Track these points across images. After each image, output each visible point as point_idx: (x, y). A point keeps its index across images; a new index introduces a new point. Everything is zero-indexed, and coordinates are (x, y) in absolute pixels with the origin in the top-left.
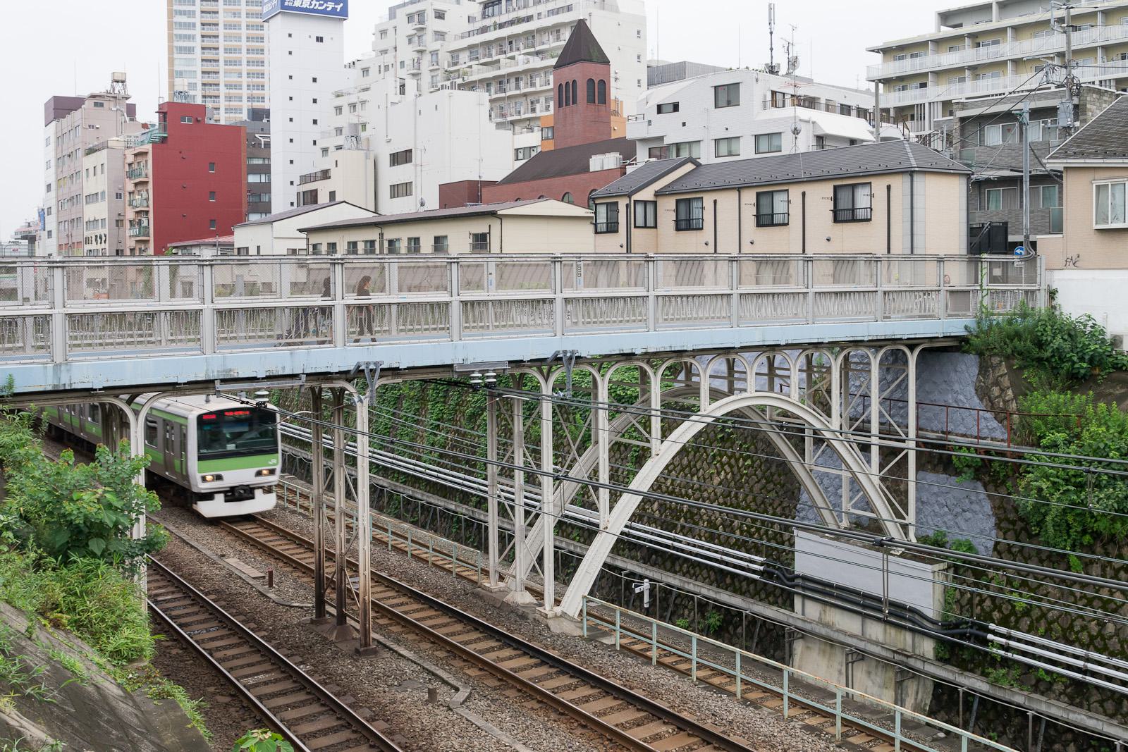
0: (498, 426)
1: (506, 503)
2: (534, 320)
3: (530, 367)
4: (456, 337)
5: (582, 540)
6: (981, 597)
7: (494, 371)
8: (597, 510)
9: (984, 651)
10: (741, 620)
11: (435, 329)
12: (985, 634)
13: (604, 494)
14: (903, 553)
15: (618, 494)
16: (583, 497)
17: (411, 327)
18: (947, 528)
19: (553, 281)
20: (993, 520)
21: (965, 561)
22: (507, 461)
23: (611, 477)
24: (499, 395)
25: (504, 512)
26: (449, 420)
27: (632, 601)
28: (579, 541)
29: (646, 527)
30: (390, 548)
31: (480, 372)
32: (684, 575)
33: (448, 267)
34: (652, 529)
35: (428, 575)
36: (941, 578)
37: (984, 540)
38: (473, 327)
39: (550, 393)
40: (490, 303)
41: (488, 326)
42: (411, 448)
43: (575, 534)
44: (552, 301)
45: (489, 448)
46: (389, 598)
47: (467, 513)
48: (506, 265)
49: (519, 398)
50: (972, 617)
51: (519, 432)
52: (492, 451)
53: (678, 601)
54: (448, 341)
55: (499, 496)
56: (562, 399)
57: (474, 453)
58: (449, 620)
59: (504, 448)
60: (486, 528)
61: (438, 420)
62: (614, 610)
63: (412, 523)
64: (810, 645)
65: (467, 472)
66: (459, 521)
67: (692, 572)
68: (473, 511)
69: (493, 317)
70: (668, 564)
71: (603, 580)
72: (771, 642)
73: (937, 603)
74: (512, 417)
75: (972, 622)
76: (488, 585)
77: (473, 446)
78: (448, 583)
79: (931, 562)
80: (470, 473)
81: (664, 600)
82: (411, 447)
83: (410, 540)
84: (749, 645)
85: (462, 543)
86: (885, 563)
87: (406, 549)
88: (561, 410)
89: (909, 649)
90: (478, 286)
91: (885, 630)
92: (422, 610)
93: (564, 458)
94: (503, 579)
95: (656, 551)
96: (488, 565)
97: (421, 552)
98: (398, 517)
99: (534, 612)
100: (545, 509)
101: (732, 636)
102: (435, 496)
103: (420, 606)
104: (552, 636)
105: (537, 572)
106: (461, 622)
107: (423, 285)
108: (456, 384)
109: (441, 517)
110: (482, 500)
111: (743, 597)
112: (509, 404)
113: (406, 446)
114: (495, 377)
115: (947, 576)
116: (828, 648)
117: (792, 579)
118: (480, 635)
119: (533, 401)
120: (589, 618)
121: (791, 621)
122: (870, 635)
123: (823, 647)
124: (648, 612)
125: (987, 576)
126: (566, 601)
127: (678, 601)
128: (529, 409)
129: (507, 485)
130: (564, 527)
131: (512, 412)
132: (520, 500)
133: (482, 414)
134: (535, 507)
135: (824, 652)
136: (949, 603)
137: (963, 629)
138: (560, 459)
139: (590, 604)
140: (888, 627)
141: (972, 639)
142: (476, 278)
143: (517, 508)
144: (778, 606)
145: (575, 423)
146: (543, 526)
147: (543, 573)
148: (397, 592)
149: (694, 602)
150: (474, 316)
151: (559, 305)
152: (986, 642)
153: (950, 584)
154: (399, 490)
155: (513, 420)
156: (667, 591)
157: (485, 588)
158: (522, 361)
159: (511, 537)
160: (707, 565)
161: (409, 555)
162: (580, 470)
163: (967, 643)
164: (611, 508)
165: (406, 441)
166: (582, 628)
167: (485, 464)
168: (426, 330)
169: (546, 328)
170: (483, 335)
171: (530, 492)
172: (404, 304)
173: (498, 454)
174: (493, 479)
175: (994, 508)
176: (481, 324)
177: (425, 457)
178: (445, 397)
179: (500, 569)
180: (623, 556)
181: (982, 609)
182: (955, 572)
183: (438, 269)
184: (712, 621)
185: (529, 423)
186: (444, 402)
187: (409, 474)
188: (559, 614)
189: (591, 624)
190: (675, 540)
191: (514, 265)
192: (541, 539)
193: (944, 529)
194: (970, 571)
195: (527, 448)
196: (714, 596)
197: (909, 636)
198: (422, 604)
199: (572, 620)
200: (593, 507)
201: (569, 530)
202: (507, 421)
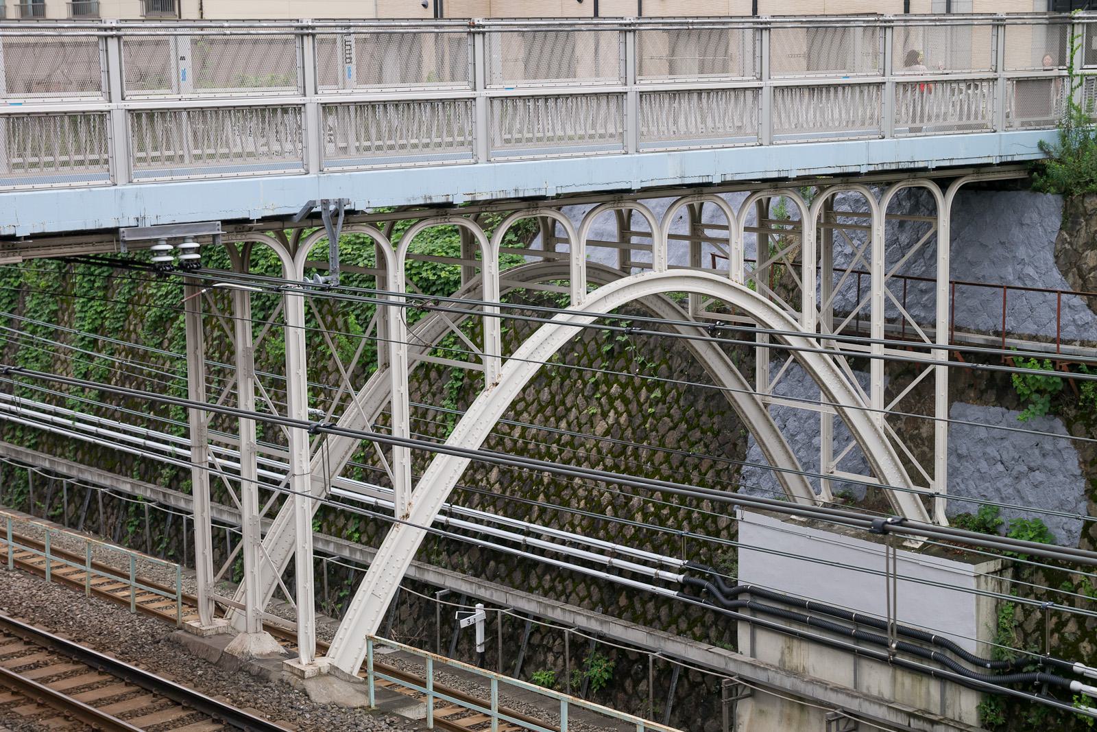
0: (206, 340)
1: (225, 477)
2: (267, 144)
3: (262, 231)
4: (121, 177)
5: (364, 539)
6: (1060, 618)
7: (196, 239)
8: (389, 485)
9: (1064, 710)
10: (646, 668)
11: (81, 163)
12: (1066, 681)
13: (402, 457)
14: (925, 544)
15: (428, 455)
16: (365, 462)
17: (36, 160)
18: (1002, 499)
19: (300, 72)
20: (1082, 484)
21: (1031, 557)
22: (226, 402)
23: (414, 427)
24: (208, 283)
25: (222, 492)
26: (116, 330)
27: (454, 644)
28: (359, 541)
29: (477, 513)
30: (11, 565)
31: (169, 241)
32: (545, 594)
33: (102, 45)
34: (489, 515)
35: (85, 611)
36: (990, 586)
37: (1064, 520)
38: (154, 159)
39: (300, 277)
40: (184, 114)
41: (182, 157)
42: (44, 382)
43: (351, 528)
44: (298, 109)
45: (191, 379)
46: (13, 655)
47: (153, 497)
48: (212, 42)
49: (243, 289)
50: (1043, 651)
51: (246, 349)
52: (197, 386)
53: (536, 639)
54: (106, 186)
55: (212, 466)
56: (322, 289)
57: (164, 390)
58: (125, 690)
59: (219, 377)
60: (190, 523)
61: (95, 330)
62: (423, 660)
63: (51, 518)
64: (765, 708)
65: (150, 424)
66: (139, 511)
67: (560, 587)
68: (164, 495)
69: (190, 138)
70: (518, 576)
71: (403, 608)
72: (697, 706)
73: (983, 628)
74: (231, 322)
75: (1044, 662)
76: (195, 624)
77: (162, 378)
78: (120, 623)
79: (974, 559)
80: (158, 426)
81: (511, 638)
82: (44, 381)
83: (48, 549)
84: (658, 709)
85: (145, 552)
86: (891, 562)
87: (42, 566)
88: (319, 306)
89: (935, 709)
90: (160, 82)
91: (894, 679)
92: (74, 673)
93: (329, 395)
94: (224, 612)
95: (496, 554)
96: (194, 589)
97: (70, 570)
98: (24, 508)
99: (280, 667)
100: (297, 486)
101: (630, 697)
102: (94, 469)
103: (70, 668)
104: (314, 709)
105: (284, 598)
106: (147, 691)
107: (54, 79)
108: (126, 264)
109: (105, 506)
110: (182, 474)
111: (648, 629)
112: (225, 298)
113: (35, 381)
114: (197, 251)
115: (1000, 583)
116: (796, 713)
117: (735, 596)
118: (183, 714)
119: (272, 296)
120: (378, 674)
121: (732, 668)
122: (868, 689)
123: (787, 710)
124: (483, 662)
125: (1070, 580)
126: (335, 647)
127: (536, 639)
128: (263, 308)
129: (227, 446)
130: (331, 518)
131: (232, 314)
132: (250, 471)
133: (177, 318)
134: (277, 483)
135: (789, 719)
136: (1005, 630)
137: (1029, 673)
138: (322, 397)
139: (381, 650)
140: (899, 673)
141: (1045, 690)
142: (156, 66)
143: (245, 485)
144: (710, 643)
145: (348, 330)
146: (294, 515)
147: (295, 598)
148: (26, 643)
149: (563, 640)
150: (154, 137)
151: (311, 116)
152: (1068, 695)
153: (1006, 595)
154: (25, 460)
155: (233, 329)
156: (517, 622)
157: (189, 630)
158: (247, 221)
159: (237, 538)
160: (585, 575)
161: (48, 576)
162: (358, 415)
163: (1035, 697)
164: (415, 481)
165: (35, 369)
166: (366, 693)
167: (185, 409)
168: (64, 164)
169: (290, 159)
170: (172, 173)
171: (269, 457)
172: (19, 117)
173: (208, 390)
174: (200, 436)
175: (1083, 462)
176: (167, 153)
177: (72, 399)
178: (106, 288)
179: (217, 596)
180: (439, 564)
181: (1062, 639)
182: (1016, 575)
183: (83, 50)
184: (595, 671)
185: (263, 332)
186: (105, 298)
187: (44, 431)
188: (324, 671)
189: (383, 685)
190: (528, 533)
191: (226, 42)
192: (290, 541)
193: (996, 501)
194: (1041, 573)
195: (262, 378)
196: (599, 628)
197: (934, 688)
198: (75, 663)
199: (348, 679)
200: (384, 480)
201: (341, 521)
202: (223, 330)
